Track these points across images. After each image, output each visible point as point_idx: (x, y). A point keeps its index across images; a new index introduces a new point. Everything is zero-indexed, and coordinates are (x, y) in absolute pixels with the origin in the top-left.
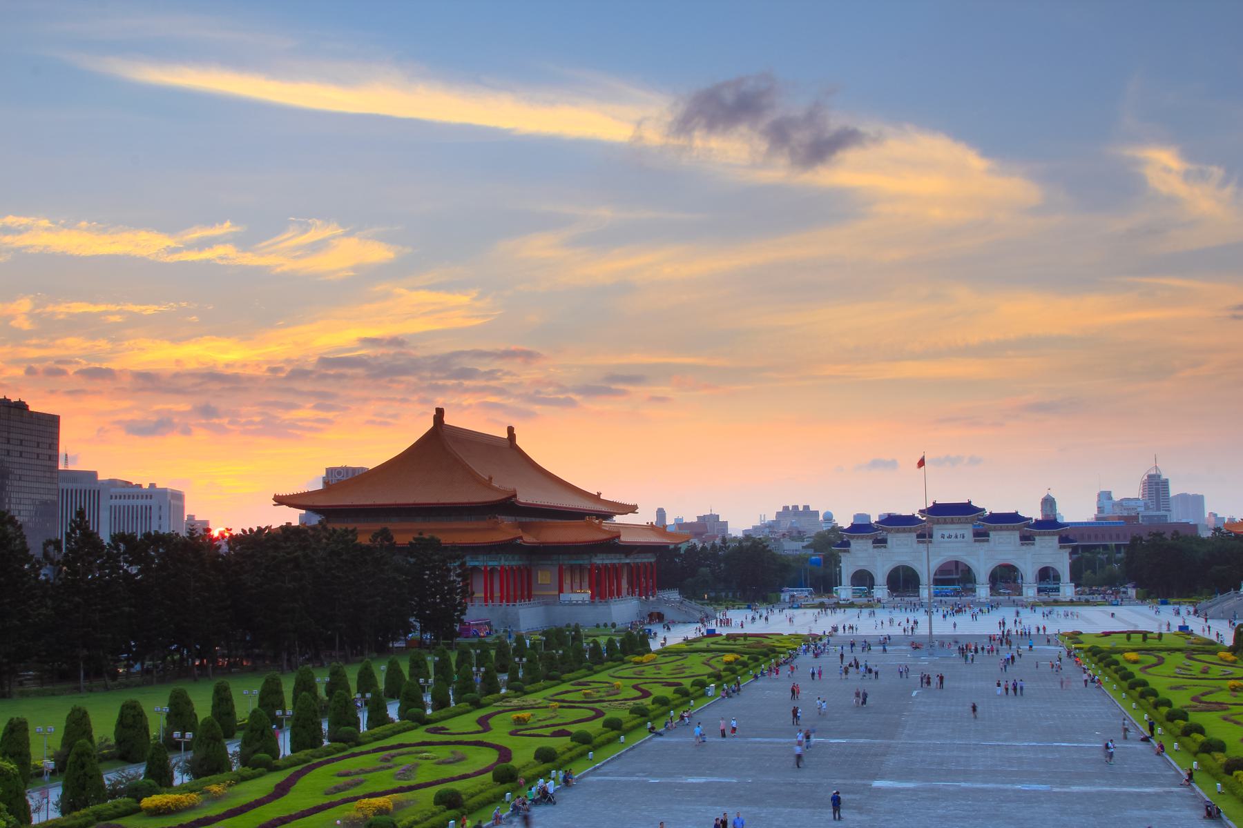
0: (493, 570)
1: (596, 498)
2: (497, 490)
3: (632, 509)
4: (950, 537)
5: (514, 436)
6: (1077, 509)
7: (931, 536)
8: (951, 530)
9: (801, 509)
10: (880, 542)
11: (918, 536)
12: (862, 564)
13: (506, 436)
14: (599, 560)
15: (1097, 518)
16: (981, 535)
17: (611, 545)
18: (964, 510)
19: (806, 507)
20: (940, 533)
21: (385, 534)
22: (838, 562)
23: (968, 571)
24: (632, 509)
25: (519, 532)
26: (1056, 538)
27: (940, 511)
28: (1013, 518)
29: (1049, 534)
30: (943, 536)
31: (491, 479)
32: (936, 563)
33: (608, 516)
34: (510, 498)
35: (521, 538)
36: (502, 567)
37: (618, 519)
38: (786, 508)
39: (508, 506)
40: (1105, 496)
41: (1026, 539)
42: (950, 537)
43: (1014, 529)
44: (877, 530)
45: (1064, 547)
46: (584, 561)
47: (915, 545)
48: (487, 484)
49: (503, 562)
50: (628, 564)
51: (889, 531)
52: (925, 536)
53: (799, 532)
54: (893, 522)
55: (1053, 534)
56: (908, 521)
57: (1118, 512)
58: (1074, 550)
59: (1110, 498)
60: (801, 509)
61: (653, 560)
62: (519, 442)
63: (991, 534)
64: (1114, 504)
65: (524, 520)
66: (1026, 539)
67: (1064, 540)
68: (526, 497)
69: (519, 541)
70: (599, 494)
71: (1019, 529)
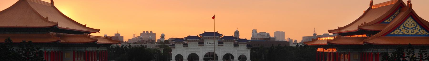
0: (48, 52)
1: (85, 26)
2: (50, 22)
3: (98, 31)
4: (210, 44)
5: (53, 2)
6: (246, 35)
7: (203, 43)
8: (211, 41)
9: (149, 32)
10: (186, 45)
11: (199, 43)
12: (179, 53)
13: (50, 2)
14: (88, 49)
15: (252, 38)
16: (221, 43)
17: (94, 43)
18: (216, 34)
19: (151, 32)
20: (207, 42)
21: (9, 38)
22: (171, 51)
23: (216, 55)
24: (98, 31)
25: (59, 39)
26: (246, 45)
27: (207, 35)
28: (231, 37)
29: (243, 44)
30: (207, 43)
31: (47, 18)
32: (204, 53)
33: (89, 33)
34: (56, 26)
35: (60, 41)
36: (52, 51)
37: (92, 34)
38: (144, 32)
39: (55, 28)
40: (254, 31)
41: (236, 45)
42: (210, 44)
43: (232, 41)
44: (185, 40)
45: (249, 48)
46: (83, 50)
47: (198, 46)
48: (46, 20)
49: (52, 50)
50: (97, 51)
51: (188, 41)
52: (201, 43)
53: (152, 41)
54: (191, 38)
55: (245, 43)
56: (197, 37)
57: (259, 37)
58: (252, 50)
59: (256, 32)
60: (149, 32)
61: (106, 50)
62: (55, 5)
63: (224, 43)
64: (258, 34)
65: (59, 34)
66: (236, 45)
67: (248, 46)
68: (62, 25)
69: (59, 42)
70: (86, 25)
71: (234, 41)
